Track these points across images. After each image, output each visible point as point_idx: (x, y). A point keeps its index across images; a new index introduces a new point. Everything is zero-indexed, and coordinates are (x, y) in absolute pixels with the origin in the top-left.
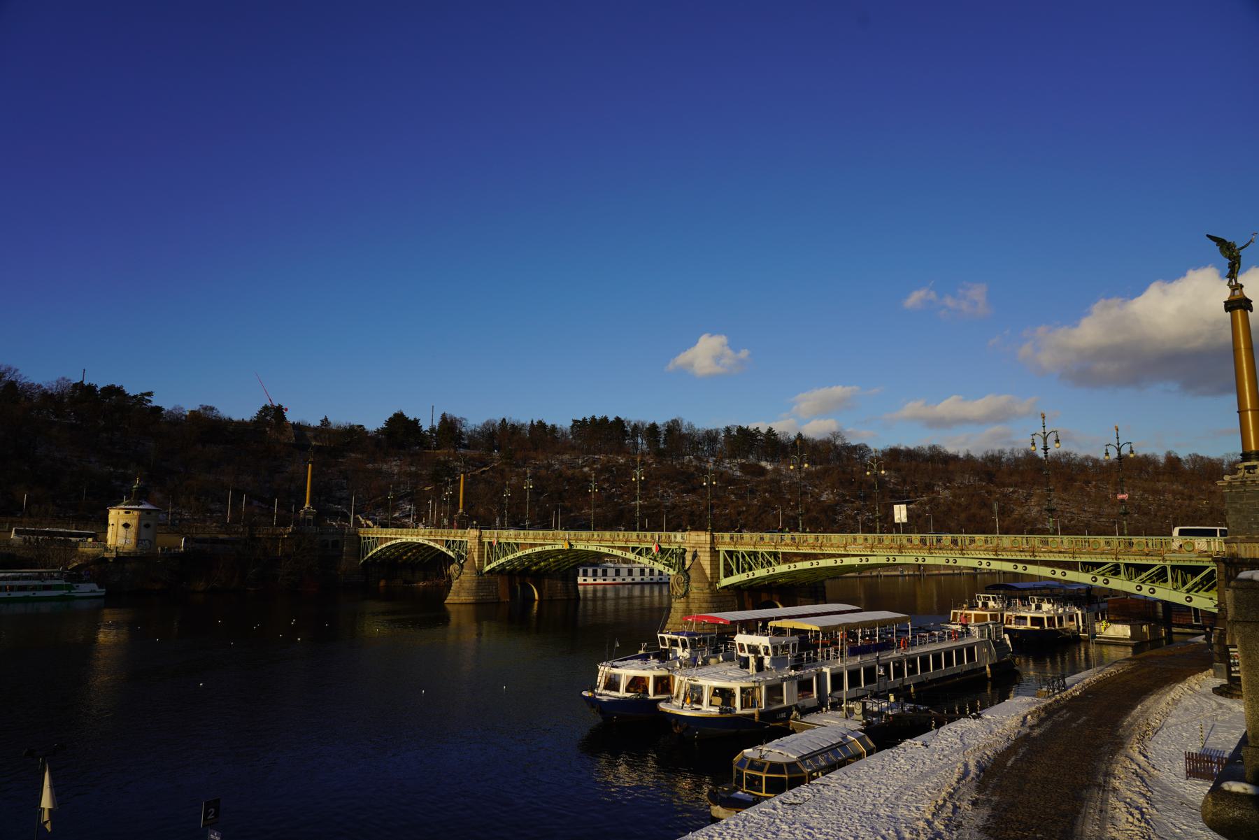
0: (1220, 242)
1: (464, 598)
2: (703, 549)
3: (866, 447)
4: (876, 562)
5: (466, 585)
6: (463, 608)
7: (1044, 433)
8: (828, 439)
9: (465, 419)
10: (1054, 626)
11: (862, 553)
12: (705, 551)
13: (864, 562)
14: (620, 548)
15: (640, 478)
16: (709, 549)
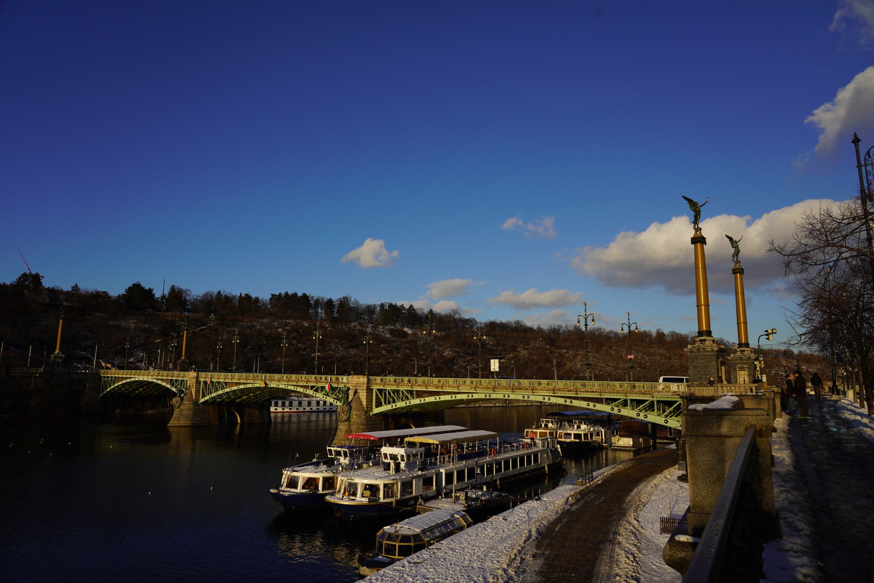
0: (690, 201)
1: (183, 422)
2: (362, 388)
3: (475, 320)
4: (478, 398)
5: (185, 412)
6: (182, 430)
7: (586, 315)
8: (450, 314)
9: (189, 290)
10: (588, 439)
11: (469, 391)
12: (363, 389)
13: (470, 397)
14: (302, 386)
15: (319, 337)
16: (365, 388)
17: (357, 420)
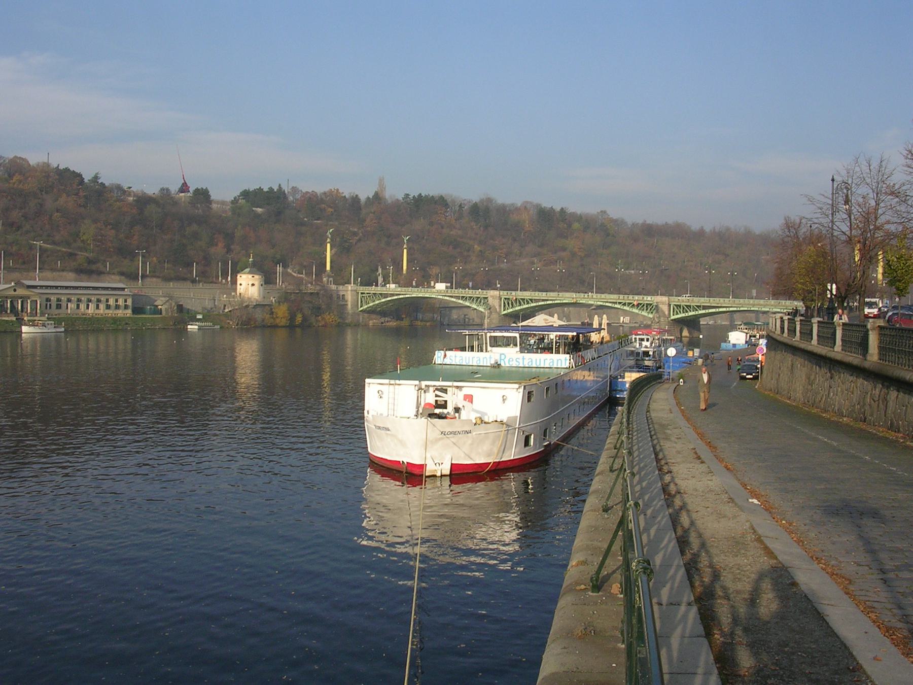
14: (610, 302)
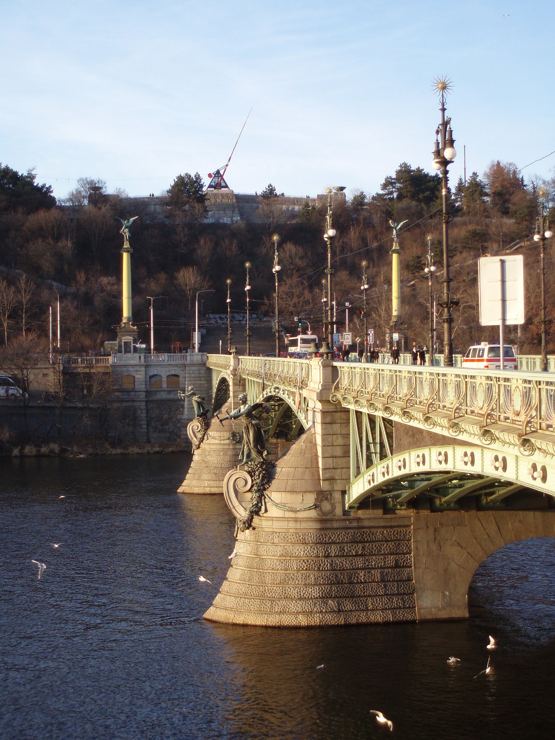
17: (284, 524)
